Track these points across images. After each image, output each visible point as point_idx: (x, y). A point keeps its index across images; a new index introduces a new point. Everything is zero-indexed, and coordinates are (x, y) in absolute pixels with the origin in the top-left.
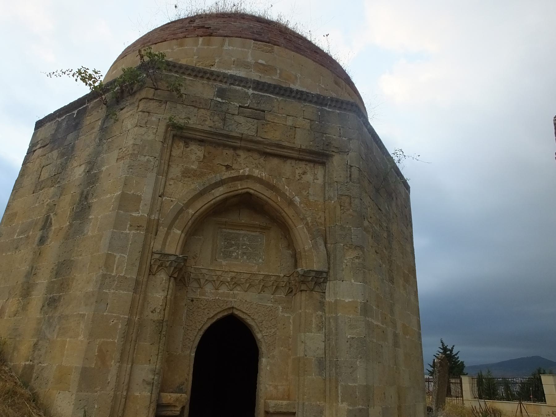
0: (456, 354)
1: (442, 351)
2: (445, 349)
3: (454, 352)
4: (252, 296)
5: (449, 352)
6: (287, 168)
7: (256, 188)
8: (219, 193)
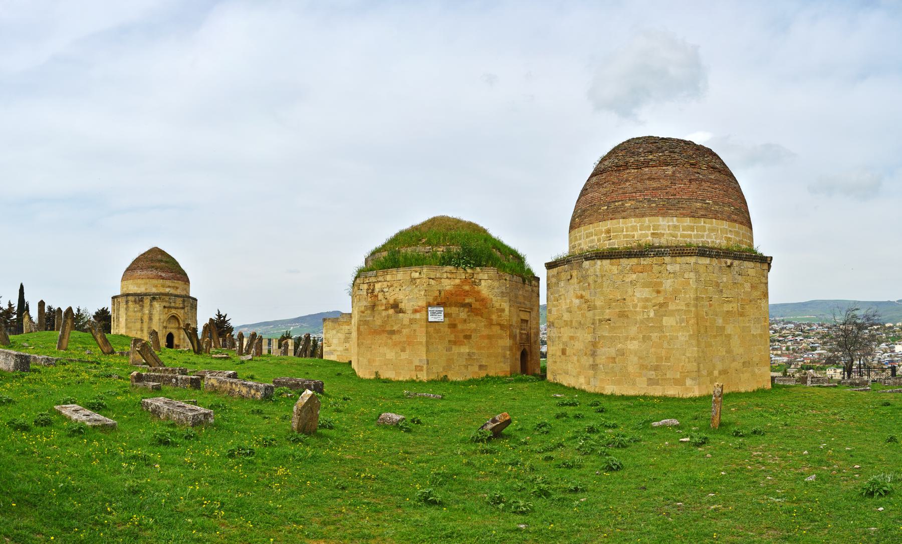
0: (228, 320)
1: (217, 317)
2: (220, 316)
3: (226, 319)
4: (173, 330)
5: (222, 318)
6: (179, 310)
7: (175, 314)
8: (170, 316)
